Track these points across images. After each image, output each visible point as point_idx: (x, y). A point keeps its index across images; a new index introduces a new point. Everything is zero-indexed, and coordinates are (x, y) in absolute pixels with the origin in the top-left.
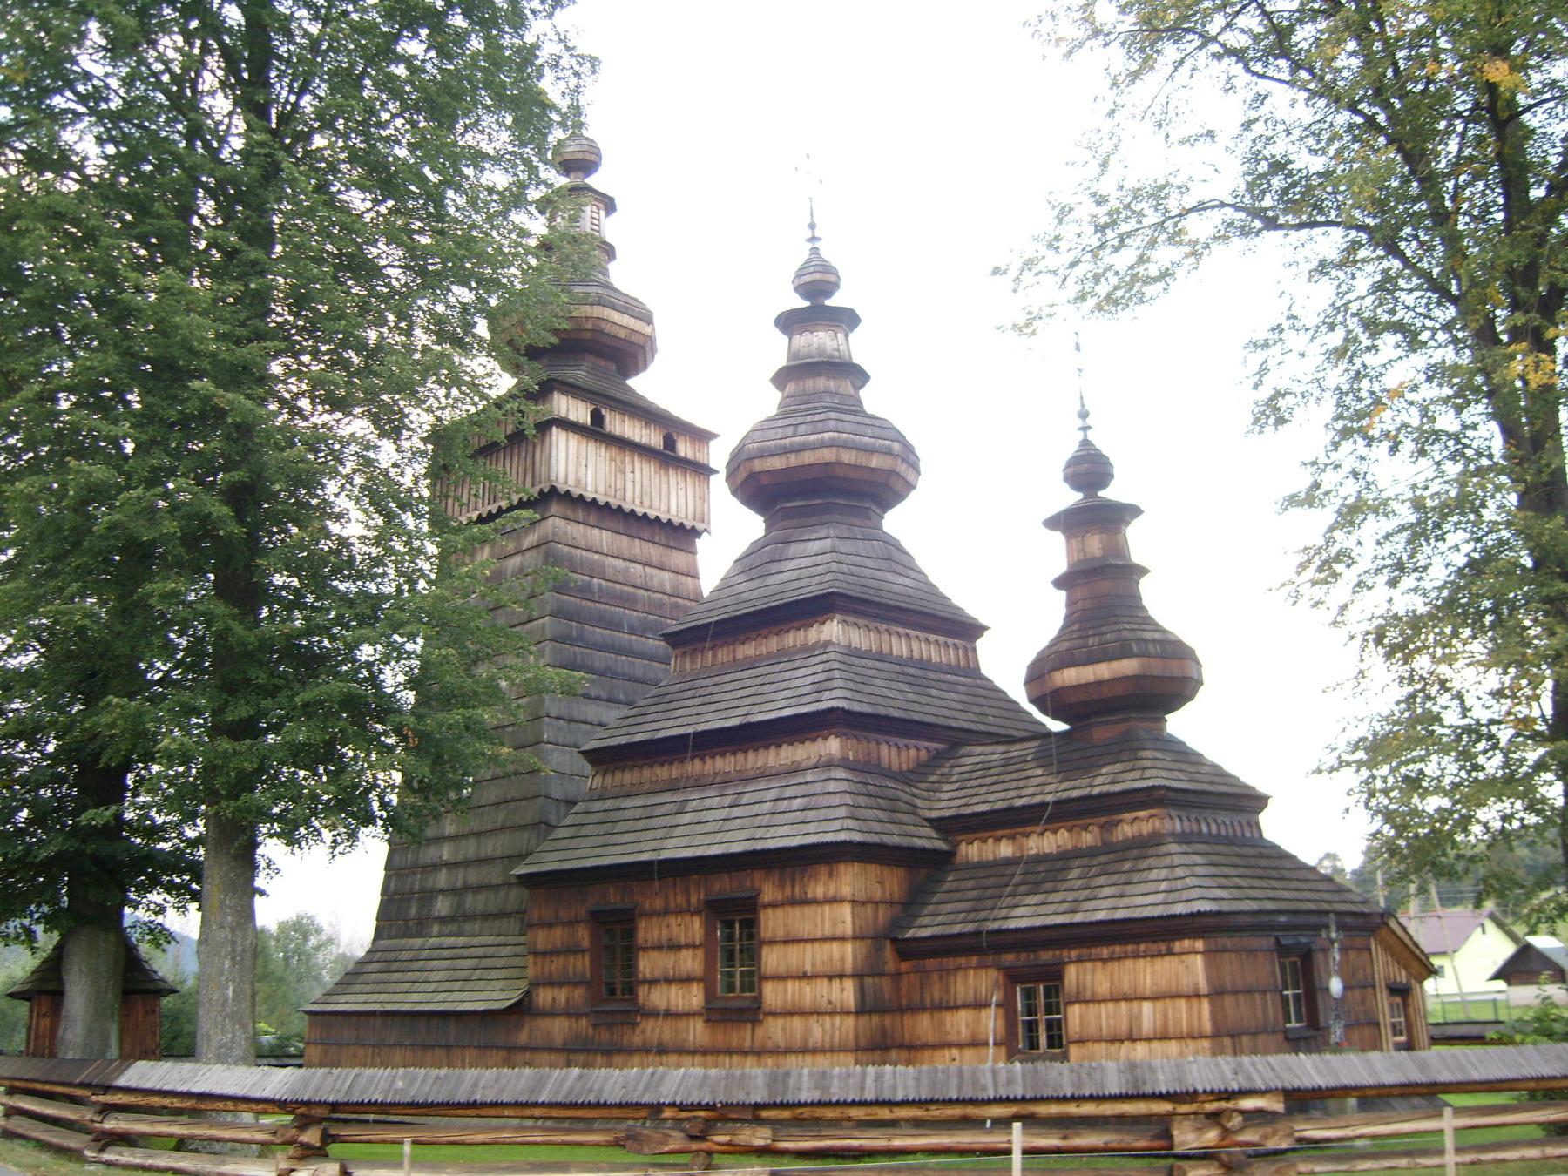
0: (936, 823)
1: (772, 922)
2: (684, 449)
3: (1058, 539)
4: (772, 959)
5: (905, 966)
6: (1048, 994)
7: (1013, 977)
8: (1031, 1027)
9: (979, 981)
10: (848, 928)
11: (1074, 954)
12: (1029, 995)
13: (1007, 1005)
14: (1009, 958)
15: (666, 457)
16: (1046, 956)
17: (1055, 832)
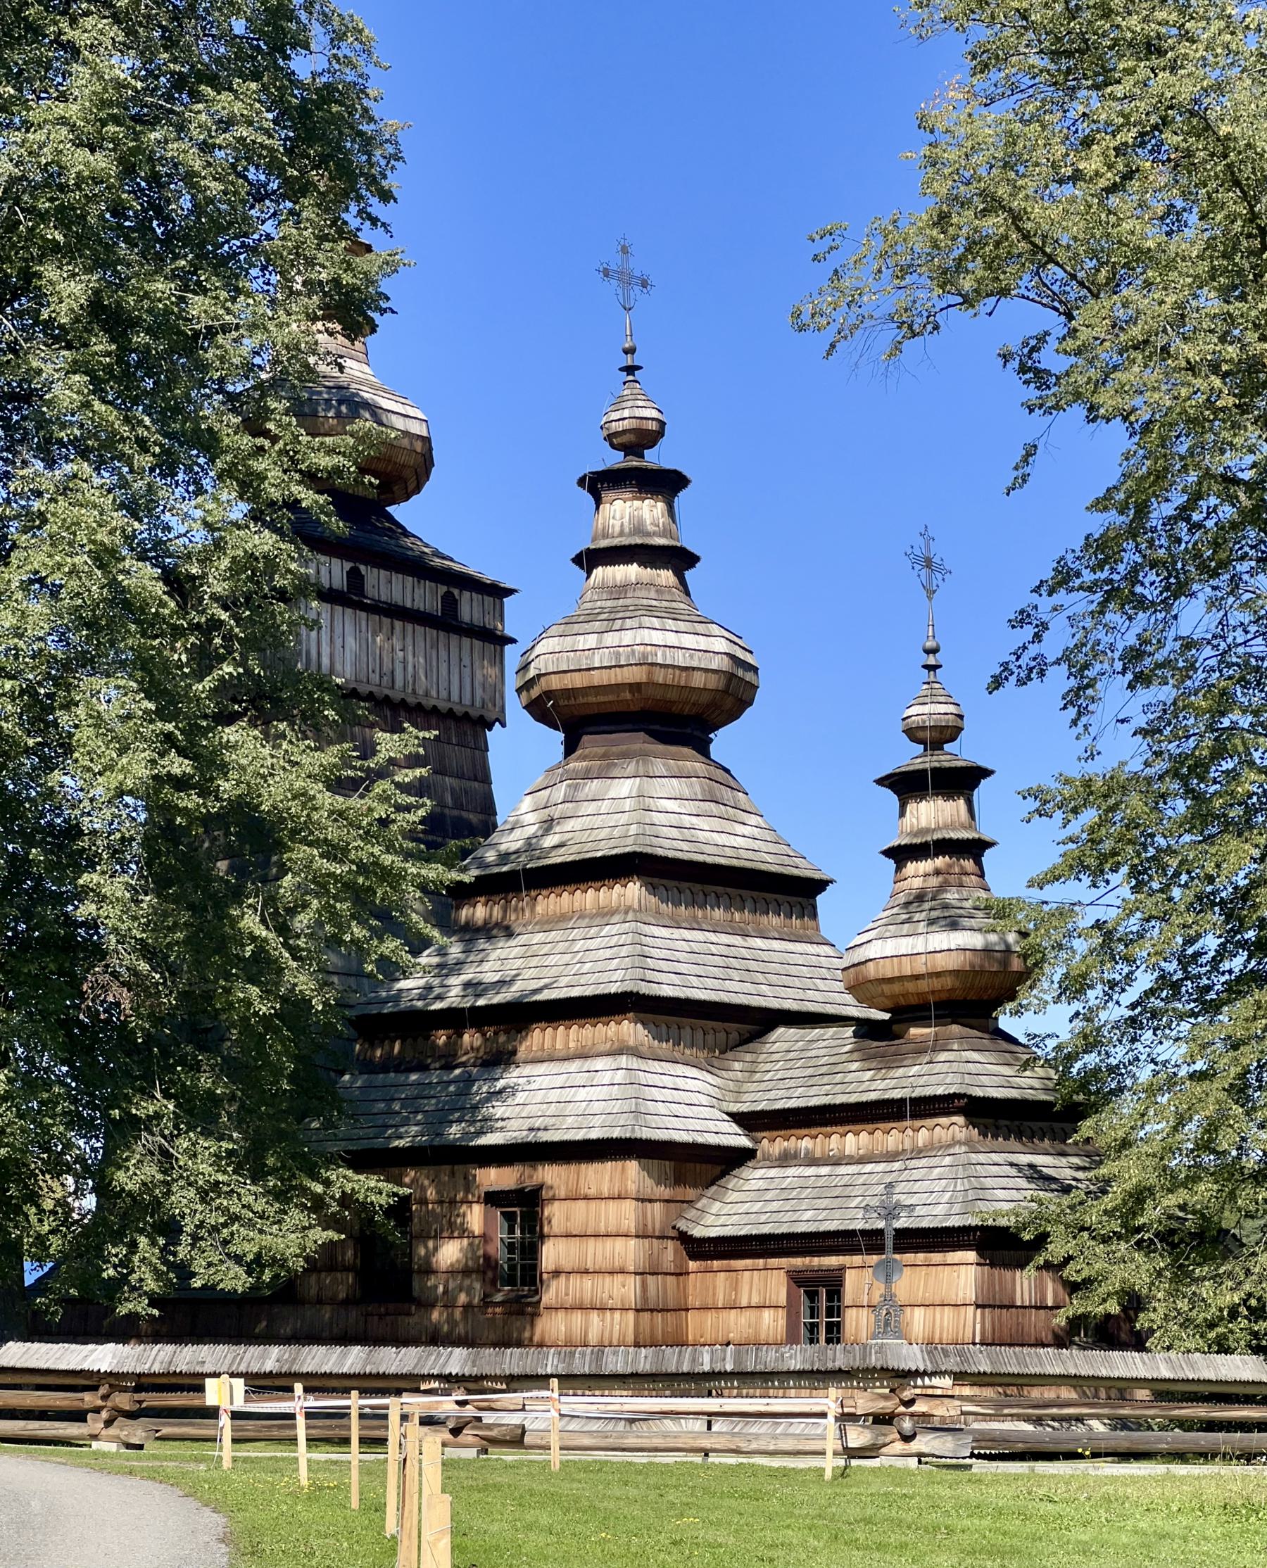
0: (737, 1118)
1: (556, 1215)
2: (470, 608)
3: (890, 798)
4: (551, 1254)
5: (692, 1265)
6: (830, 1299)
7: (797, 1279)
8: (813, 1328)
9: (767, 1283)
10: (630, 1225)
11: (857, 1259)
12: (812, 1296)
13: (791, 1308)
14: (798, 1262)
15: (445, 622)
16: (832, 1261)
17: (857, 1134)
